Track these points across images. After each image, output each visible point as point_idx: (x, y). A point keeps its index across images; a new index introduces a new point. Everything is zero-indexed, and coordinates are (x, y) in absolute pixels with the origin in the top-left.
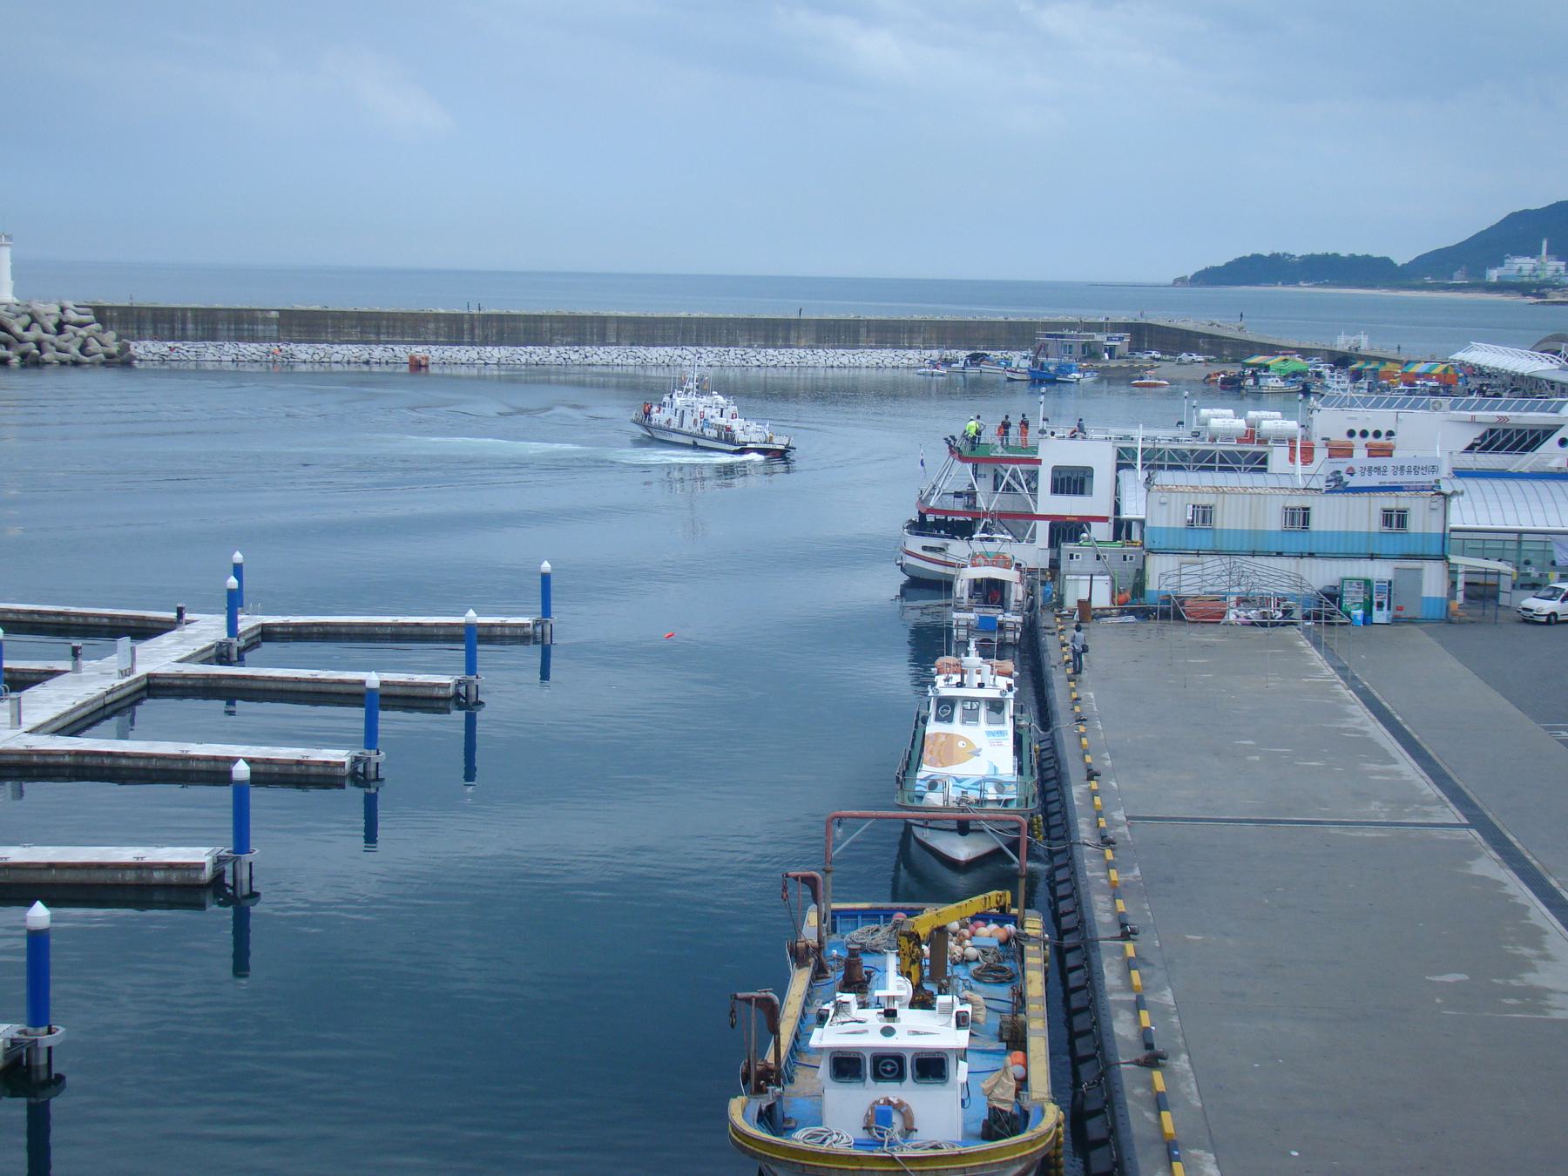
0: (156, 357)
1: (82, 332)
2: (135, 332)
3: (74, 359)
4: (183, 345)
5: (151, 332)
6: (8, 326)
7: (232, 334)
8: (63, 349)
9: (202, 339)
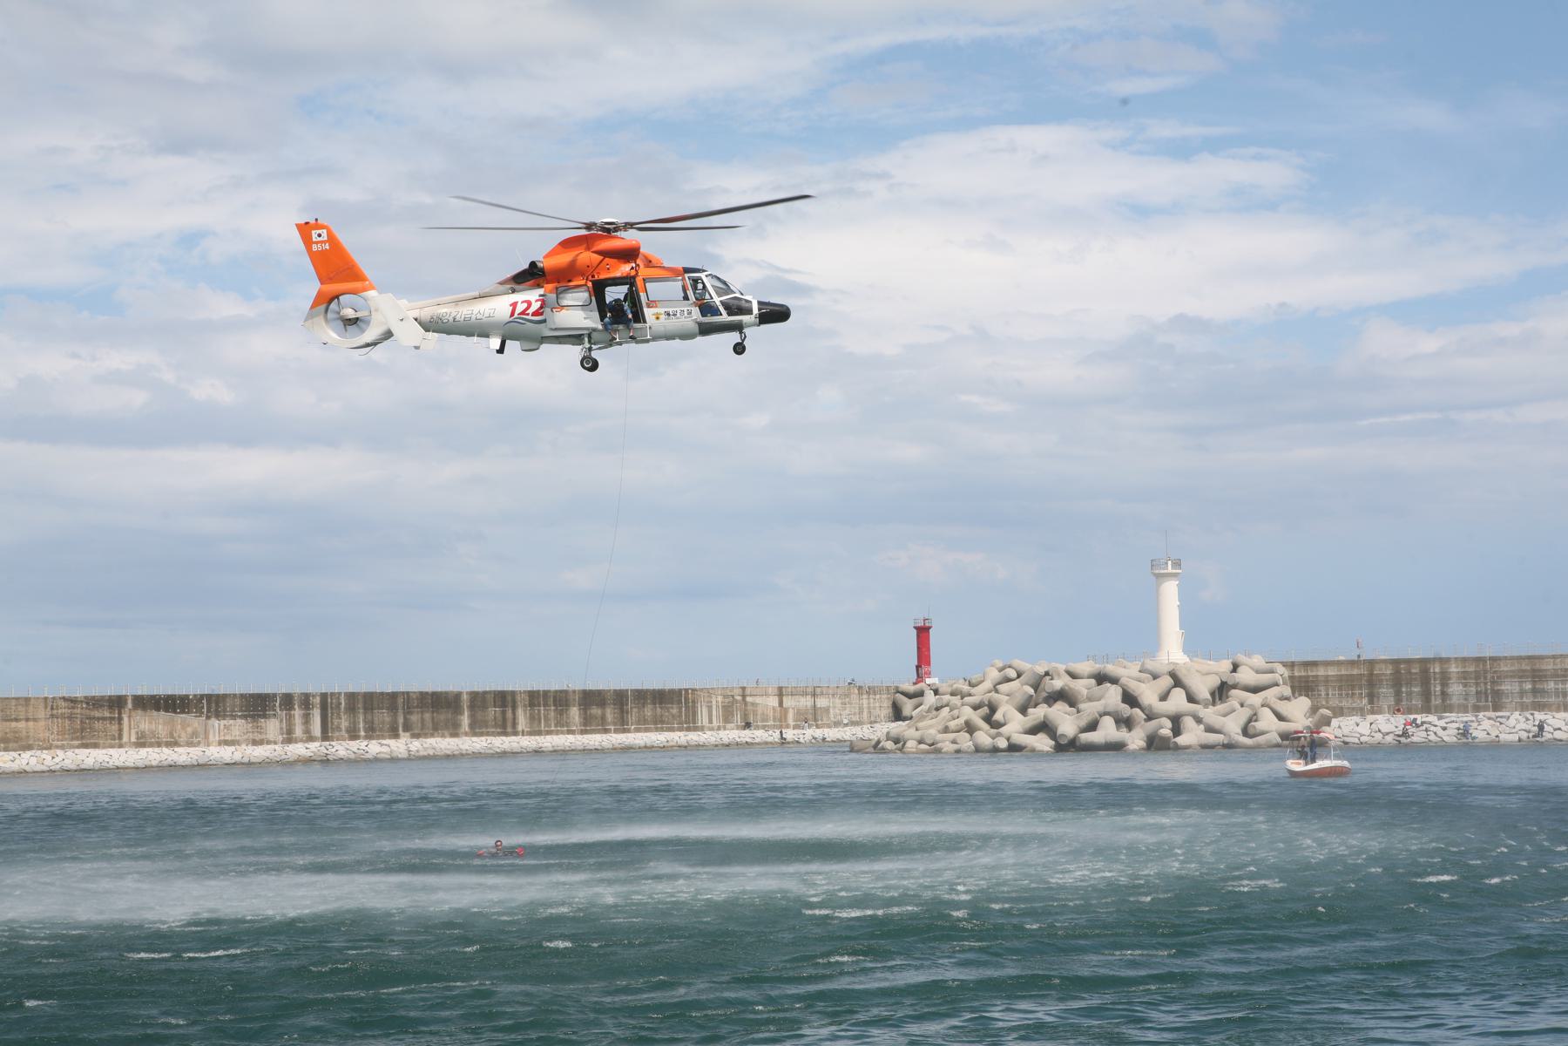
0: (1389, 739)
1: (1255, 699)
2: (1365, 701)
3: (1226, 742)
4: (1439, 719)
5: (1391, 701)
6: (1136, 694)
7: (1528, 700)
8: (1217, 726)
9: (1477, 709)
